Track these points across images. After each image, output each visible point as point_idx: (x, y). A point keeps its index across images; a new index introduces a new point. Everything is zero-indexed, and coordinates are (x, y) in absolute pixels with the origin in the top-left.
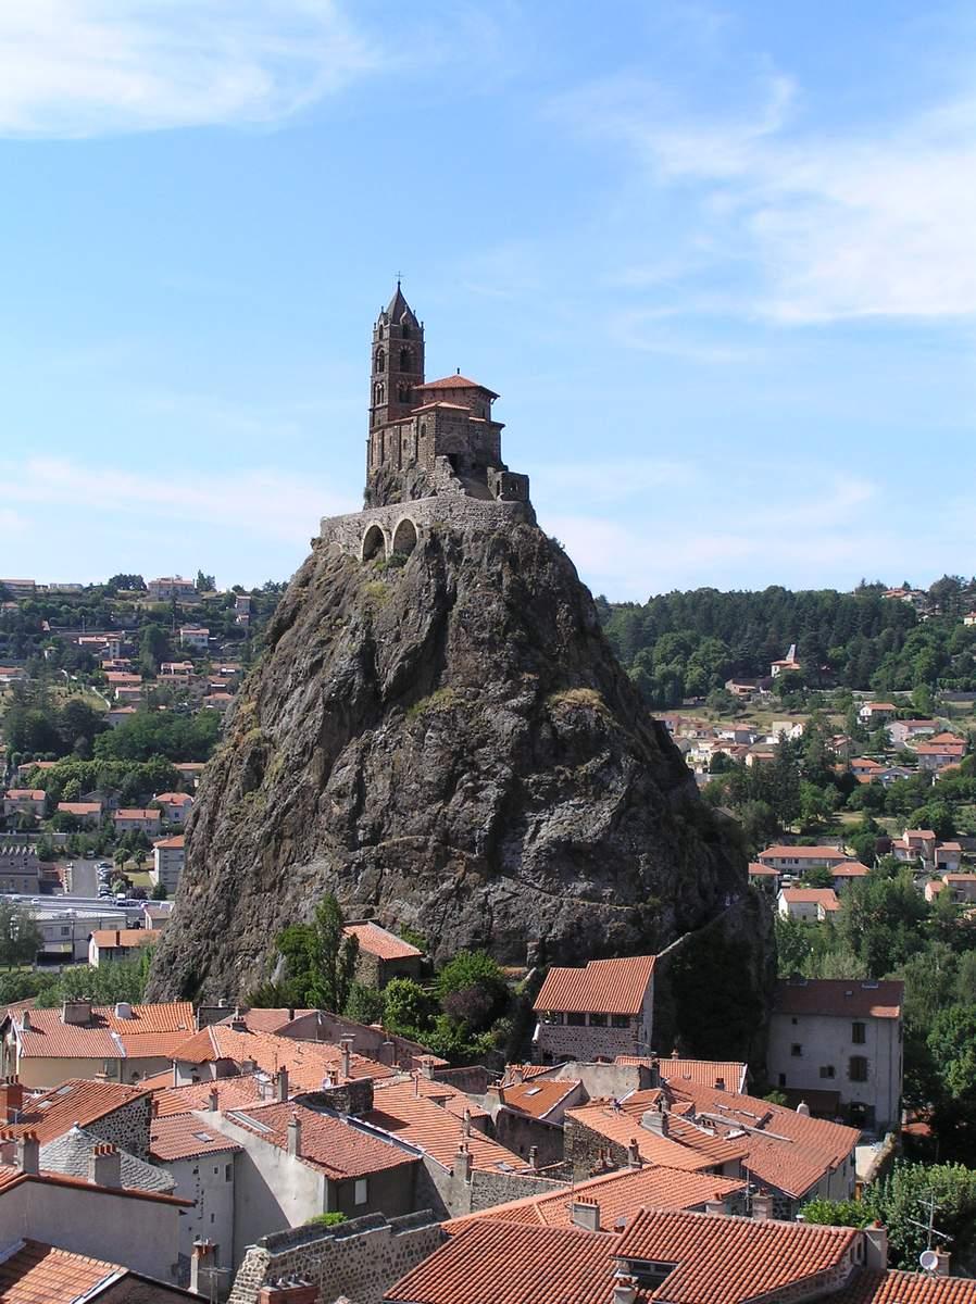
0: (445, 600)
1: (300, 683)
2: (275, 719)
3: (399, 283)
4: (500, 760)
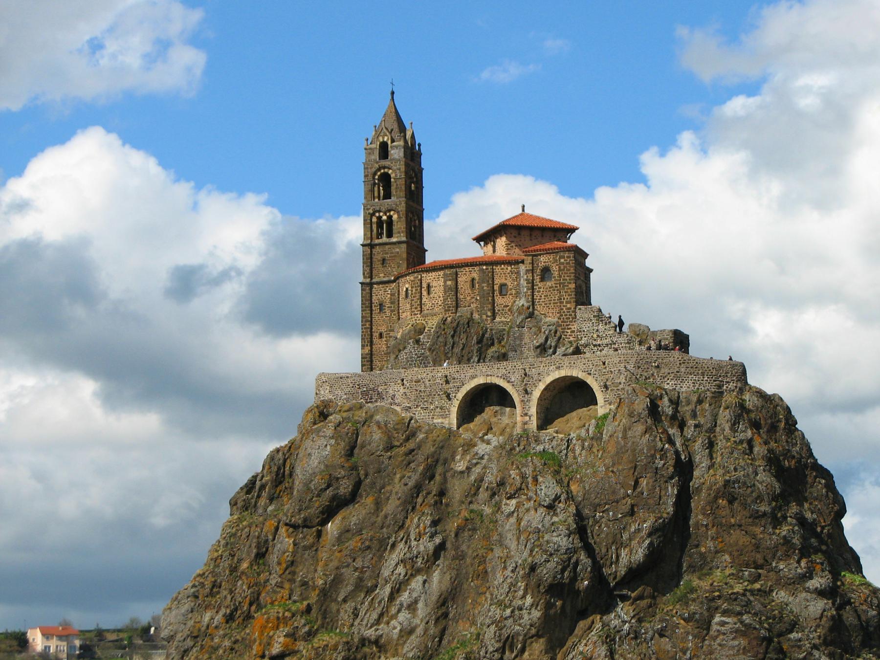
0: (684, 469)
1: (419, 571)
2: (381, 615)
3: (393, 93)
4: (815, 647)
